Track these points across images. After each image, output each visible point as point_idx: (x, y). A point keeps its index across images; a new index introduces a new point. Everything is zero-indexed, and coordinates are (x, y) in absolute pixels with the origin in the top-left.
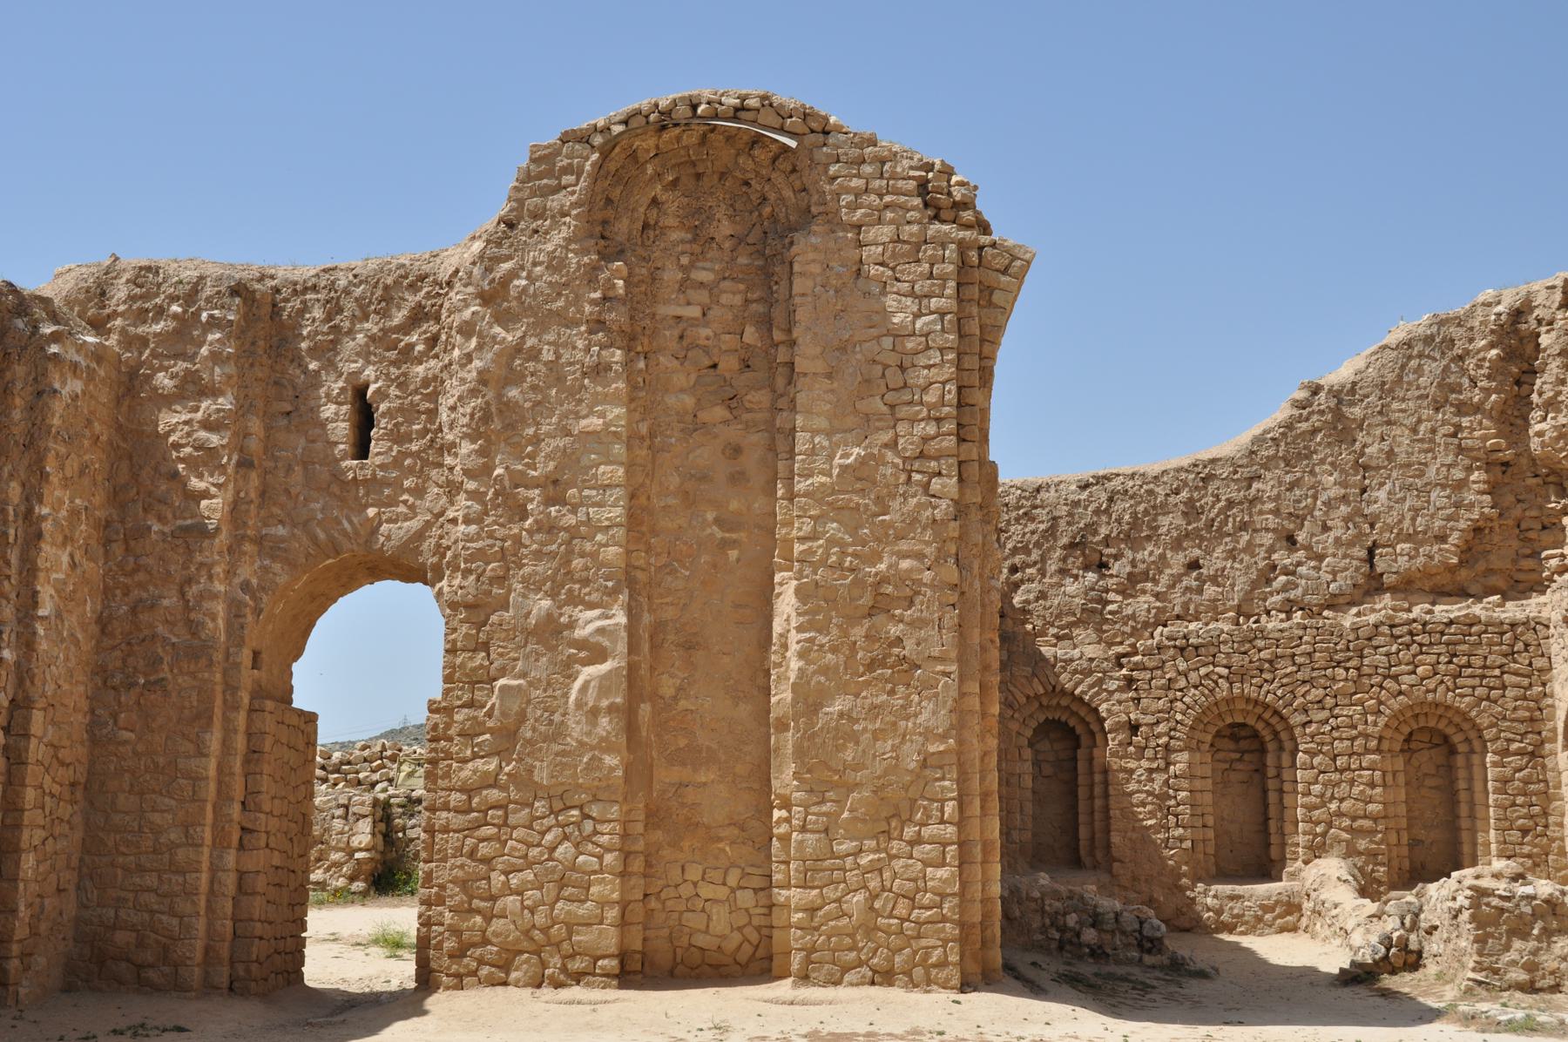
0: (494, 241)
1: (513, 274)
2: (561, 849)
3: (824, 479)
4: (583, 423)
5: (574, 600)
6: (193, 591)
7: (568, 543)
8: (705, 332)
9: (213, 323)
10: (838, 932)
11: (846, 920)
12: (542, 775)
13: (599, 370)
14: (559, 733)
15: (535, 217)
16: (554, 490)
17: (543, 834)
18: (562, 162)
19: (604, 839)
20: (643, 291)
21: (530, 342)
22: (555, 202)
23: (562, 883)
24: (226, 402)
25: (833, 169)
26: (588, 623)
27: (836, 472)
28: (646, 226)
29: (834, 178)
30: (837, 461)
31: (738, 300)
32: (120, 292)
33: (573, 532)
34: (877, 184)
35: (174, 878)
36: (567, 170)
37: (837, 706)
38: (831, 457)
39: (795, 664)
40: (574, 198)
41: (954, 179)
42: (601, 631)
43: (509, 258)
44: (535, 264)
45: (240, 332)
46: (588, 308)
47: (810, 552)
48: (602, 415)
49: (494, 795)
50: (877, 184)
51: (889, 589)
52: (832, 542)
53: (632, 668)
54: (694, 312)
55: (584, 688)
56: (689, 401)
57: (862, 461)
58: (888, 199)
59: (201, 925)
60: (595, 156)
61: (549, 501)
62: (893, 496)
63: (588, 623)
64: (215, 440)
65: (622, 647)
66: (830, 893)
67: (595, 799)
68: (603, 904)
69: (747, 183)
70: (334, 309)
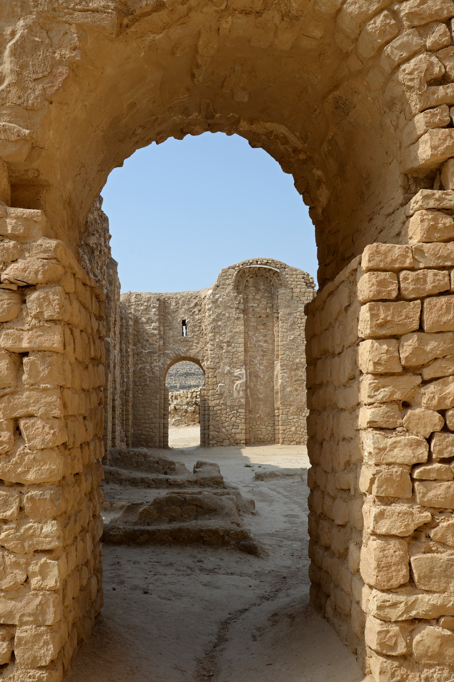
0: (215, 290)
1: (219, 297)
2: (233, 419)
3: (286, 342)
4: (235, 330)
5: (234, 367)
6: (153, 365)
7: (232, 355)
8: (258, 309)
9: (154, 307)
10: (289, 435)
11: (291, 432)
12: (229, 403)
13: (238, 319)
14: (232, 395)
15: (223, 285)
16: (229, 343)
17: (229, 415)
18: (228, 273)
19: (242, 417)
20: (246, 300)
21: (223, 313)
22: (228, 282)
23: (233, 425)
24: (157, 324)
25: (287, 276)
26: (237, 372)
27: (288, 341)
28: (245, 286)
29: (287, 278)
30: (288, 339)
31: (266, 302)
32: (133, 300)
33: (233, 353)
34: (296, 280)
35: (153, 425)
36: (230, 275)
37: (288, 389)
38: (287, 338)
39: (280, 381)
40: (232, 281)
41: (310, 277)
42: (240, 374)
43: (218, 294)
44: (224, 295)
45: (159, 309)
46: (235, 305)
47: (283, 357)
48: (239, 328)
49: (218, 408)
50: (296, 280)
51: (299, 365)
52: (287, 355)
53: (246, 381)
54: (256, 305)
55: (237, 386)
56: (255, 324)
57: (293, 339)
58: (298, 283)
59: (158, 434)
60: (236, 272)
61: (228, 346)
62: (300, 346)
63: (237, 372)
64: (156, 332)
65: (245, 377)
66: (288, 427)
67: (239, 408)
68: (242, 429)
69: (267, 278)
70: (177, 303)
